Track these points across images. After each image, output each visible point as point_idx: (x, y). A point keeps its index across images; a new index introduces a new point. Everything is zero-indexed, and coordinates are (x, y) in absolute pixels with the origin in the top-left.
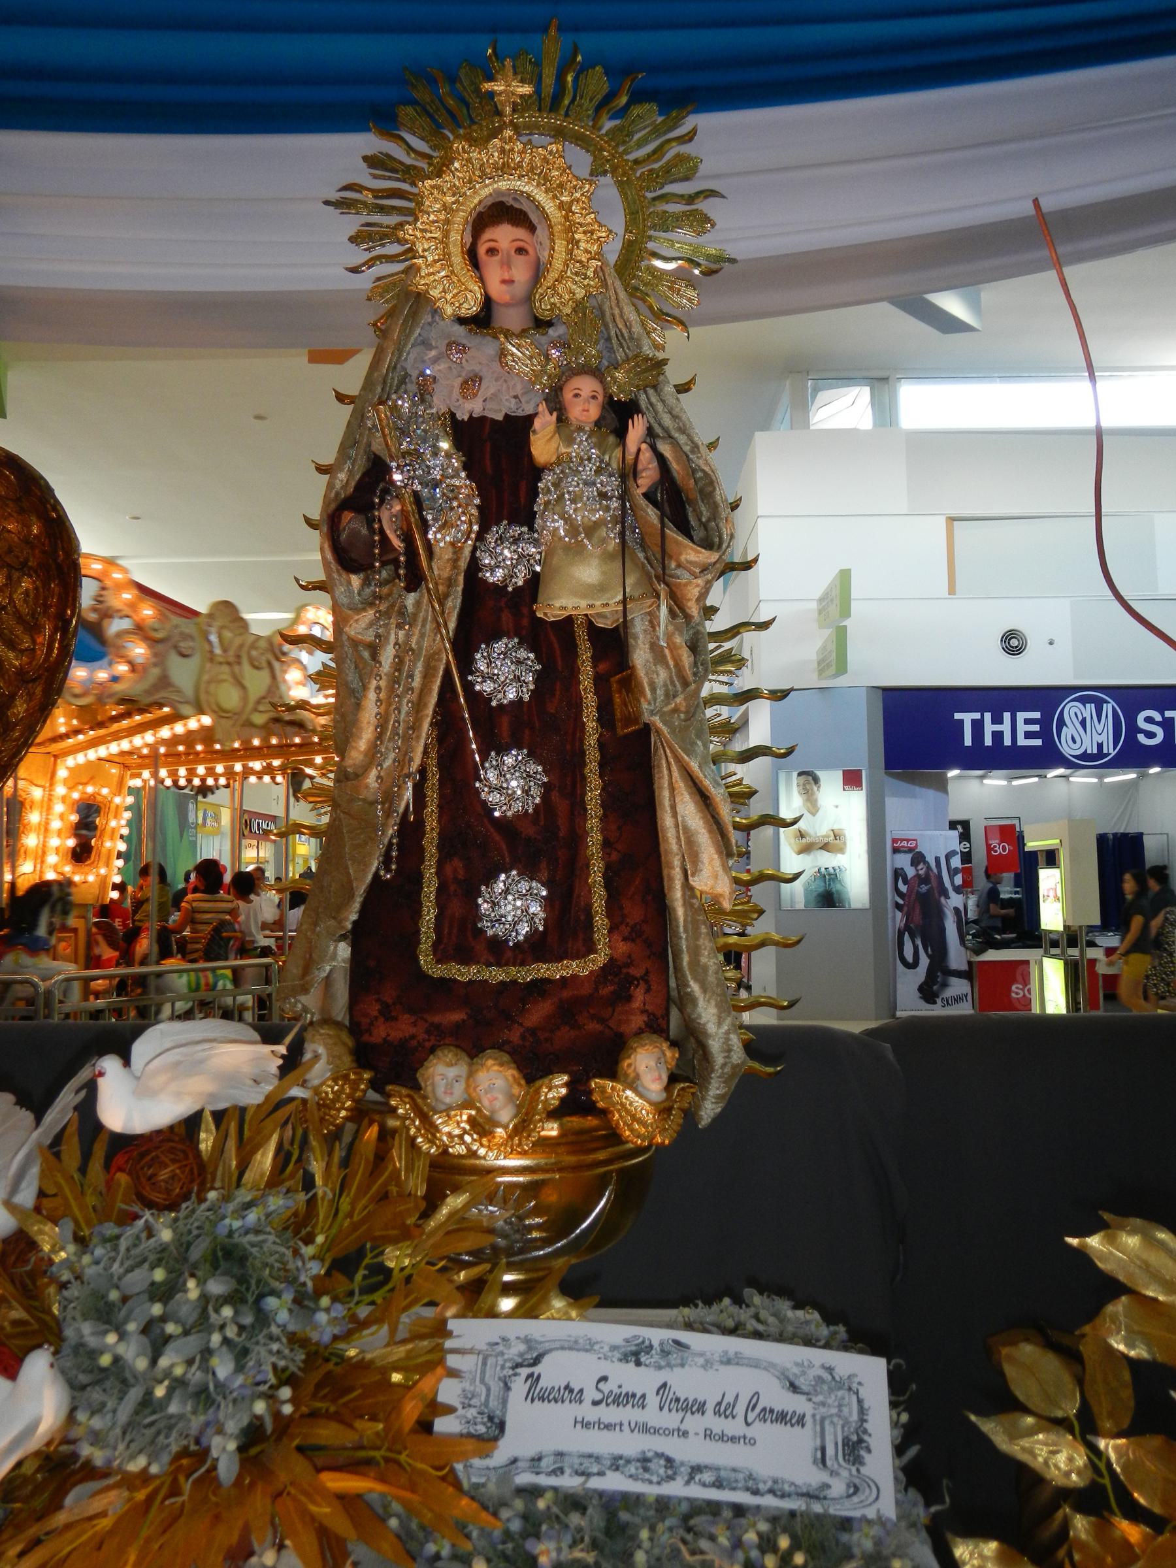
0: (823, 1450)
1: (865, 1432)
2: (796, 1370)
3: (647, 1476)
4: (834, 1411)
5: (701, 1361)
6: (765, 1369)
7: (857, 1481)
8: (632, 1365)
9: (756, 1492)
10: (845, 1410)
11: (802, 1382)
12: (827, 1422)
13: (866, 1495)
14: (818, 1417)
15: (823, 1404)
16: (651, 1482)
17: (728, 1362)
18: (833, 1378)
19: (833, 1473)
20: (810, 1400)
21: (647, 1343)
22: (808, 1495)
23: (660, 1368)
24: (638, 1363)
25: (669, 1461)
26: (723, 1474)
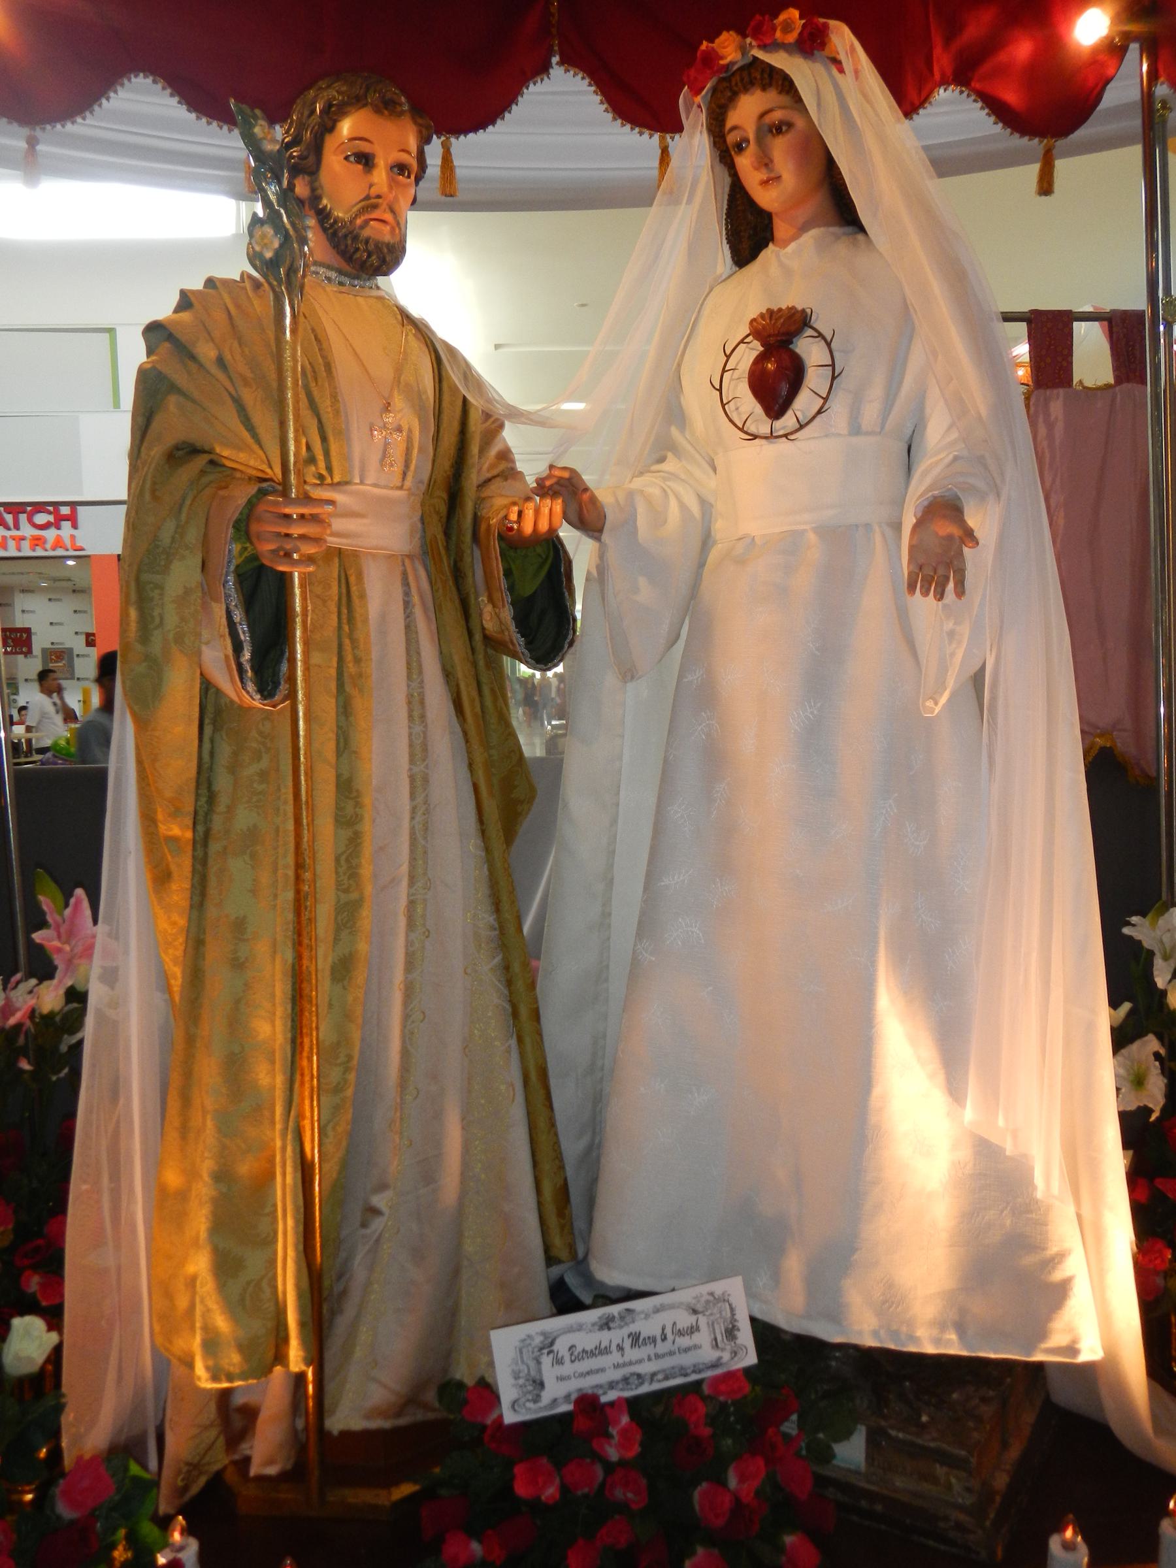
0: (716, 1339)
1: (736, 1320)
2: (694, 1301)
3: (629, 1387)
4: (718, 1315)
5: (643, 1316)
6: (678, 1307)
7: (735, 1349)
8: (606, 1330)
9: (686, 1375)
10: (724, 1313)
11: (699, 1307)
12: (715, 1325)
13: (741, 1354)
14: (710, 1323)
15: (711, 1314)
16: (632, 1389)
17: (657, 1310)
18: (715, 1298)
19: (723, 1350)
20: (704, 1315)
21: (611, 1316)
22: (714, 1366)
23: (621, 1327)
24: (609, 1329)
25: (639, 1376)
26: (668, 1372)
